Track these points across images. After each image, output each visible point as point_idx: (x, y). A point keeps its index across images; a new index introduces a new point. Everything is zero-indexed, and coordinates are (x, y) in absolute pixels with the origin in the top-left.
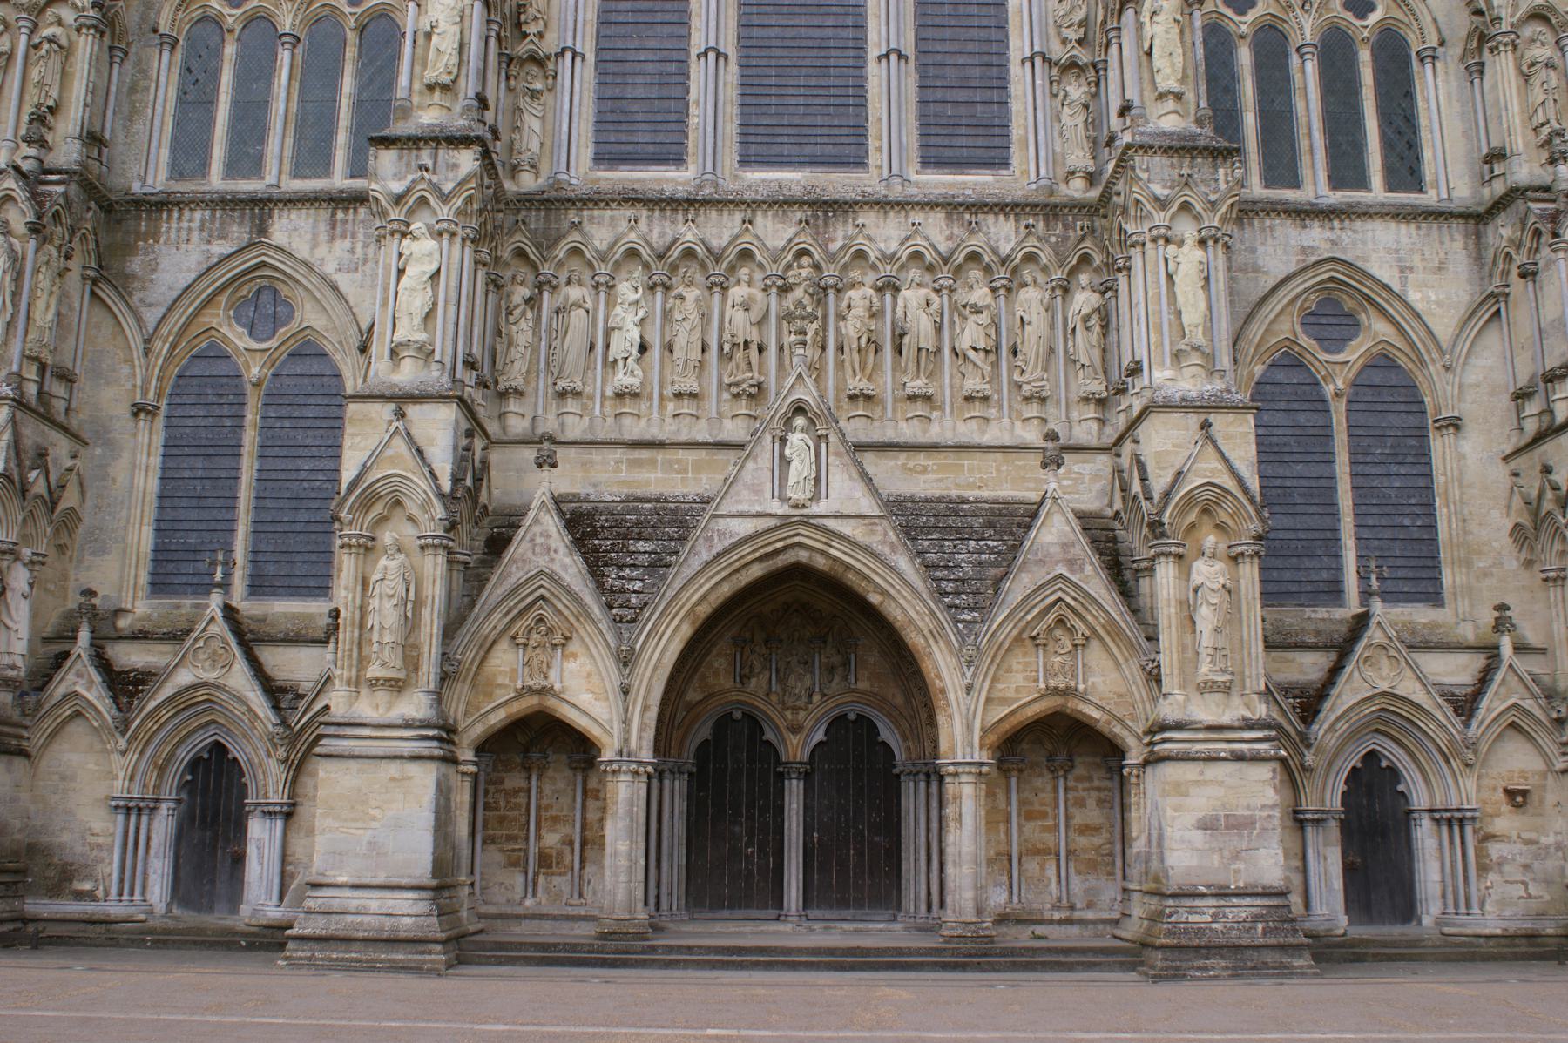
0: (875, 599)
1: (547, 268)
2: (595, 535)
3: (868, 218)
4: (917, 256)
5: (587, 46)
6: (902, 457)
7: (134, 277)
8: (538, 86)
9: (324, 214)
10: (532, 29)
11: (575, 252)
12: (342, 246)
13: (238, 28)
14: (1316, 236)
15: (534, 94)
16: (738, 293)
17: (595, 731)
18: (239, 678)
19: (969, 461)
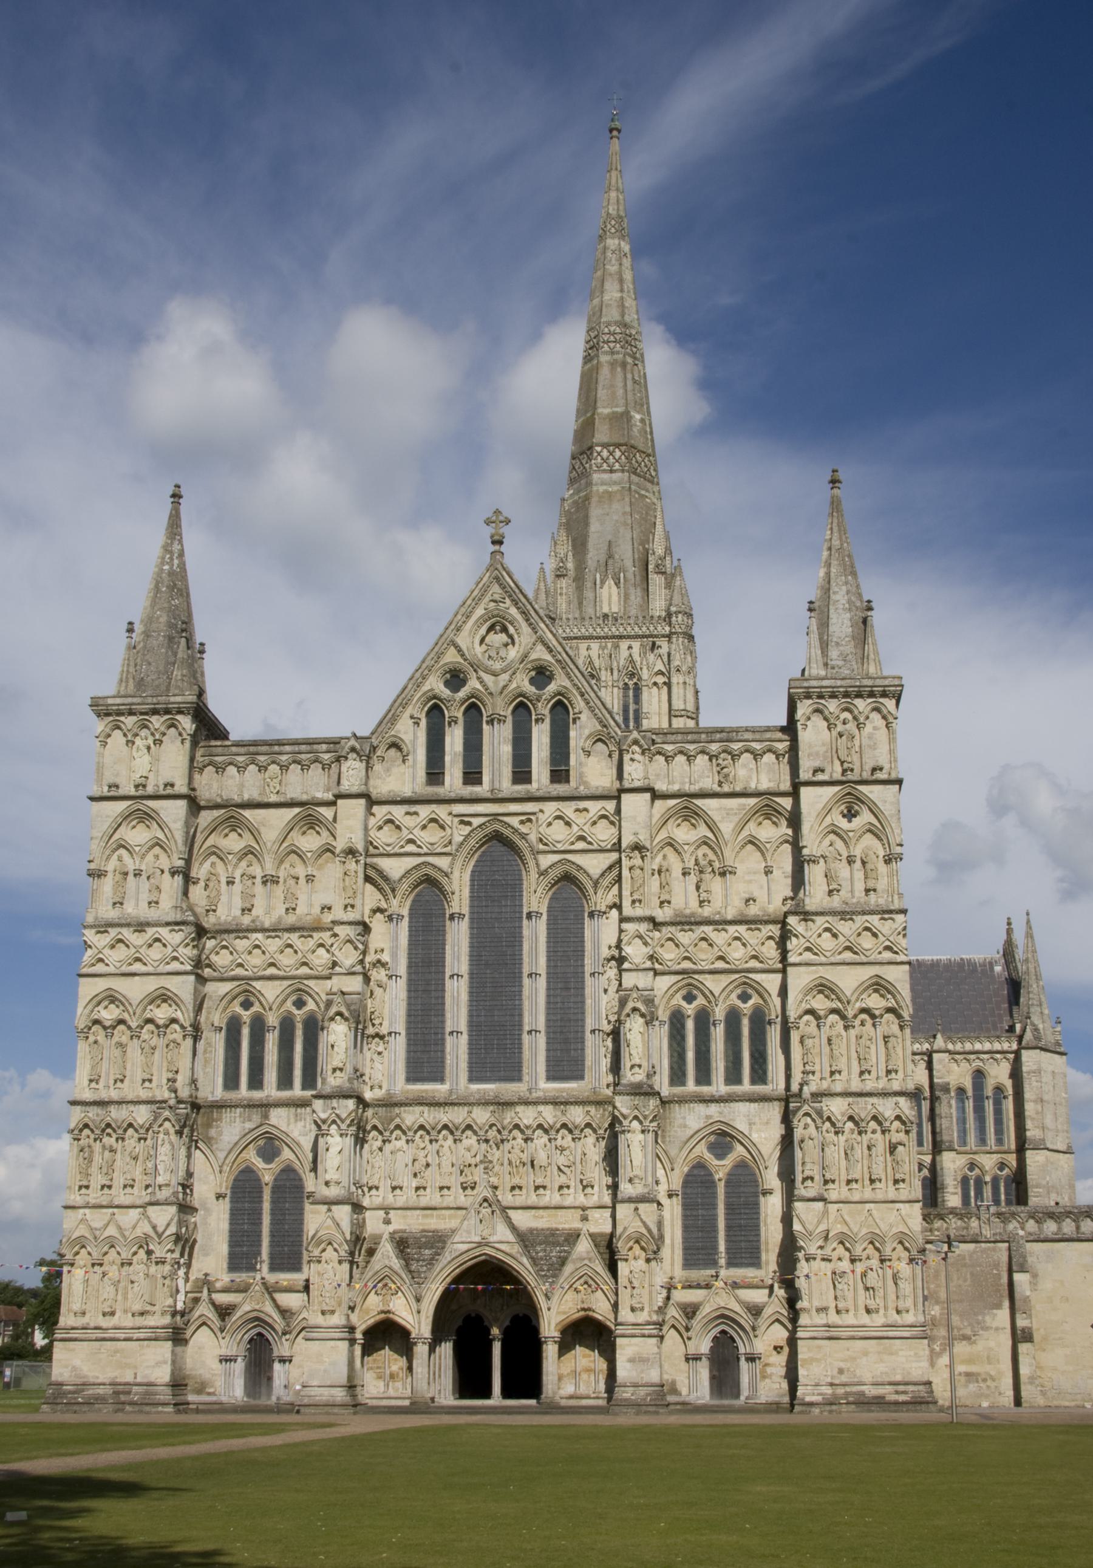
0: (515, 1273)
1: (387, 1134)
2: (408, 1247)
3: (519, 1109)
4: (540, 1126)
5: (401, 1027)
6: (533, 1211)
7: (213, 1138)
8: (380, 1049)
9: (293, 1110)
10: (376, 1022)
11: (398, 1127)
12: (300, 1124)
13: (248, 1021)
14: (713, 1109)
15: (380, 1053)
16: (466, 1142)
17: (408, 1327)
18: (269, 1308)
19: (560, 1212)
